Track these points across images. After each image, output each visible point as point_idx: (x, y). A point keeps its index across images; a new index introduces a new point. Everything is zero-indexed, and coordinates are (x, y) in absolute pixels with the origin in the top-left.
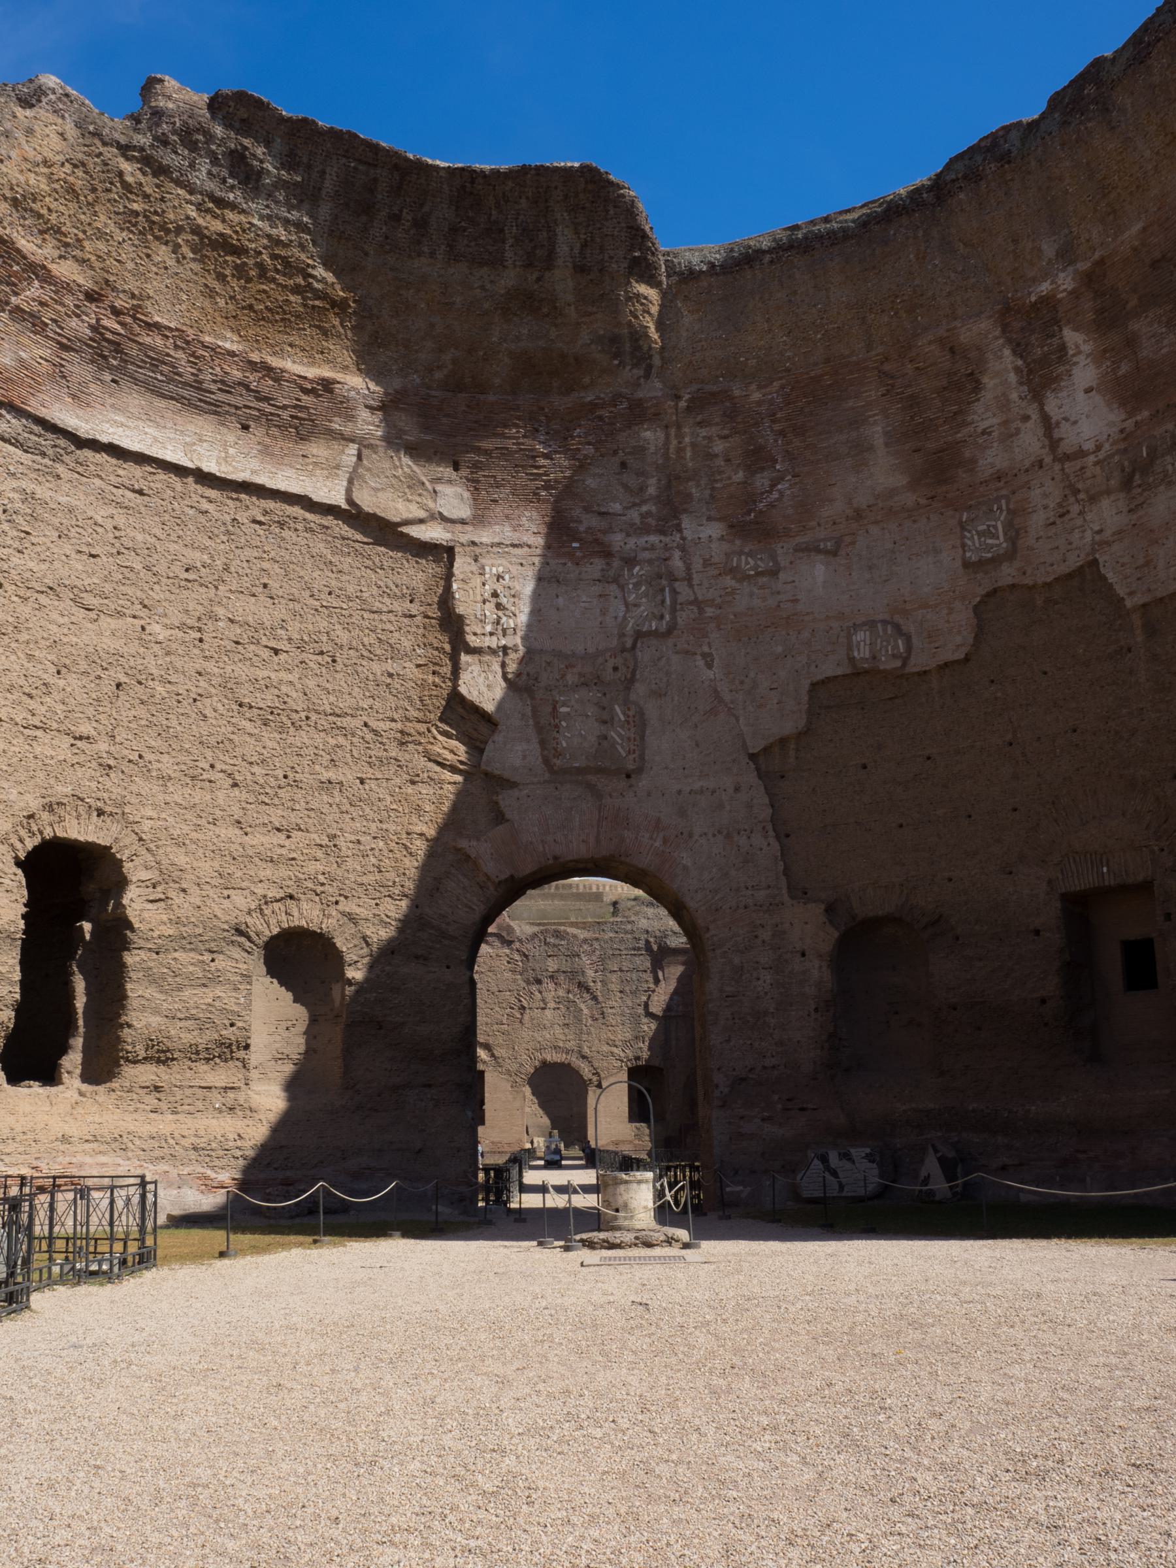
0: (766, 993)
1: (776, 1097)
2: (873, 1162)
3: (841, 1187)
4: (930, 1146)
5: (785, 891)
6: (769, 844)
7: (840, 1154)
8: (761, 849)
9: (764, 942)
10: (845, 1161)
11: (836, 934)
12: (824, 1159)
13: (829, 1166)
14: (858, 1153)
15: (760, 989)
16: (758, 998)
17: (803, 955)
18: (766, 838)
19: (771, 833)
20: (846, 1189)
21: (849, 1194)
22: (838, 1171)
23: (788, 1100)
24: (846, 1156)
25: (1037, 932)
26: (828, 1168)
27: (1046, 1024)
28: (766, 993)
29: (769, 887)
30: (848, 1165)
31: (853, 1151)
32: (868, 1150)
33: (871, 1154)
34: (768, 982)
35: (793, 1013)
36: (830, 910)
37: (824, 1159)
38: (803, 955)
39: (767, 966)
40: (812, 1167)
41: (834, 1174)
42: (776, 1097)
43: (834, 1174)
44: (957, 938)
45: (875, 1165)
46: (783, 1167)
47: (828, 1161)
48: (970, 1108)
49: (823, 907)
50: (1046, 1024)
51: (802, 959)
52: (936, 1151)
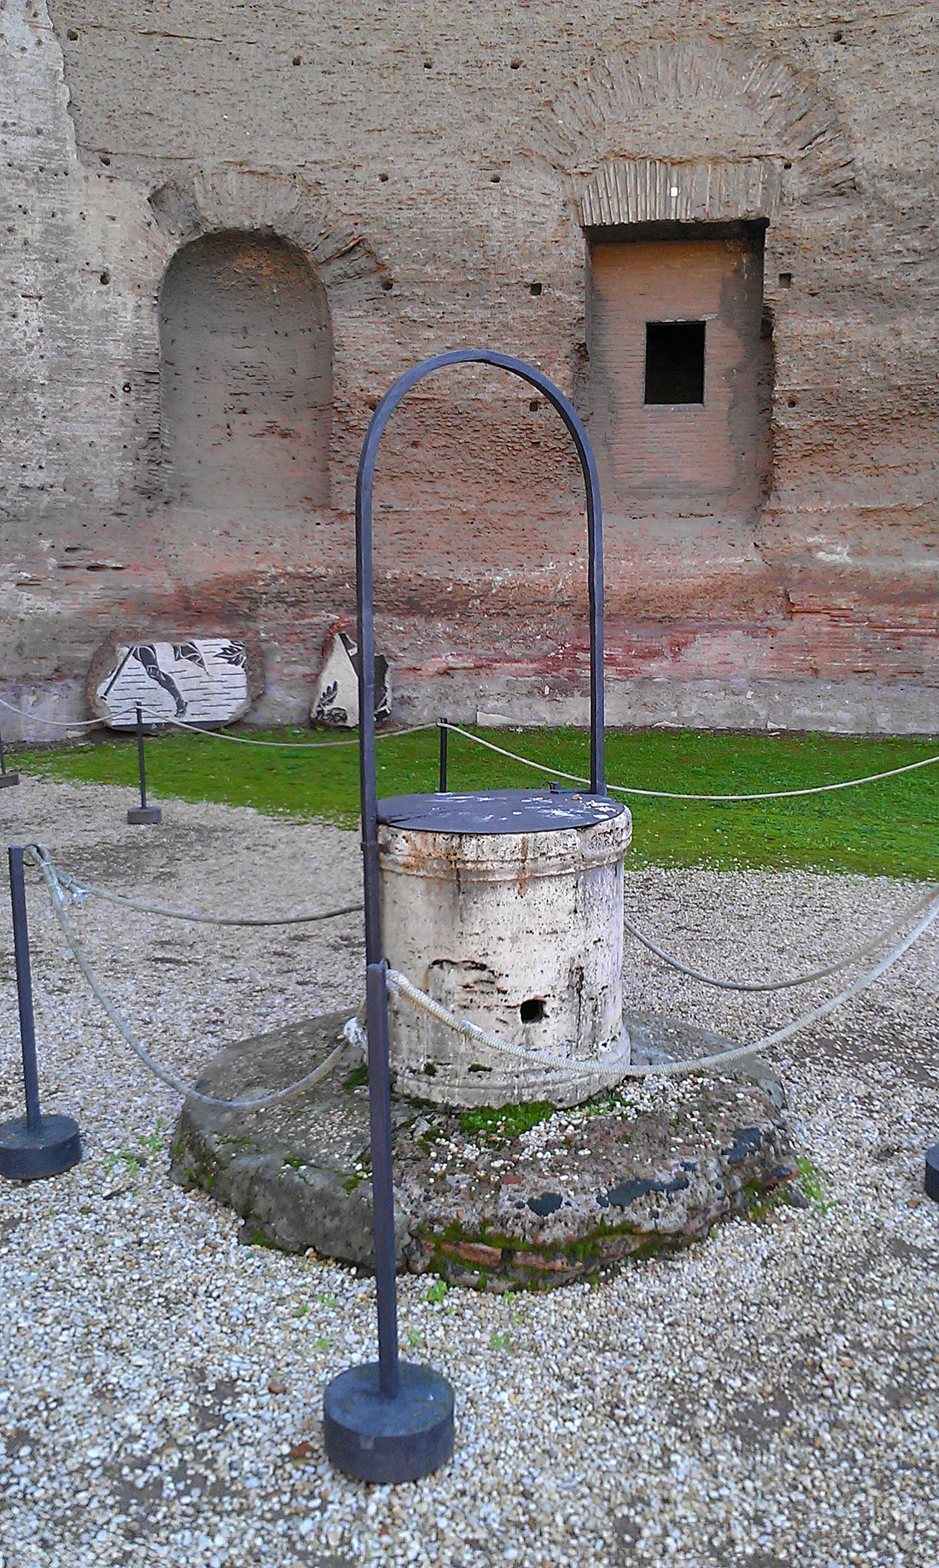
0: (30, 346)
1: (46, 544)
2: (236, 663)
3: (181, 707)
4: (337, 637)
5: (70, 147)
6: (39, 43)
7: (176, 649)
8: (23, 49)
9: (26, 243)
10: (185, 661)
11: (172, 251)
12: (147, 658)
13: (157, 669)
14: (209, 647)
15: (16, 336)
16: (13, 352)
17: (104, 280)
18: (34, 27)
19: (44, 19)
20: (189, 709)
21: (196, 719)
22: (174, 678)
23: (67, 550)
24: (188, 653)
25: (536, 289)
26: (154, 673)
27: (536, 444)
28: (30, 346)
29: (39, 132)
30: (191, 668)
31: (196, 642)
32: (226, 643)
33: (231, 649)
34: (35, 323)
35: (83, 389)
36: (155, 199)
37: (147, 658)
38: (104, 280)
39: (32, 292)
40: (124, 671)
41: (167, 683)
42: (46, 544)
43: (167, 683)
44: (388, 286)
45: (239, 668)
46: (56, 670)
47: (154, 662)
48: (389, 577)
49: (147, 193)
50: (536, 444)
51: (104, 288)
52: (348, 646)
